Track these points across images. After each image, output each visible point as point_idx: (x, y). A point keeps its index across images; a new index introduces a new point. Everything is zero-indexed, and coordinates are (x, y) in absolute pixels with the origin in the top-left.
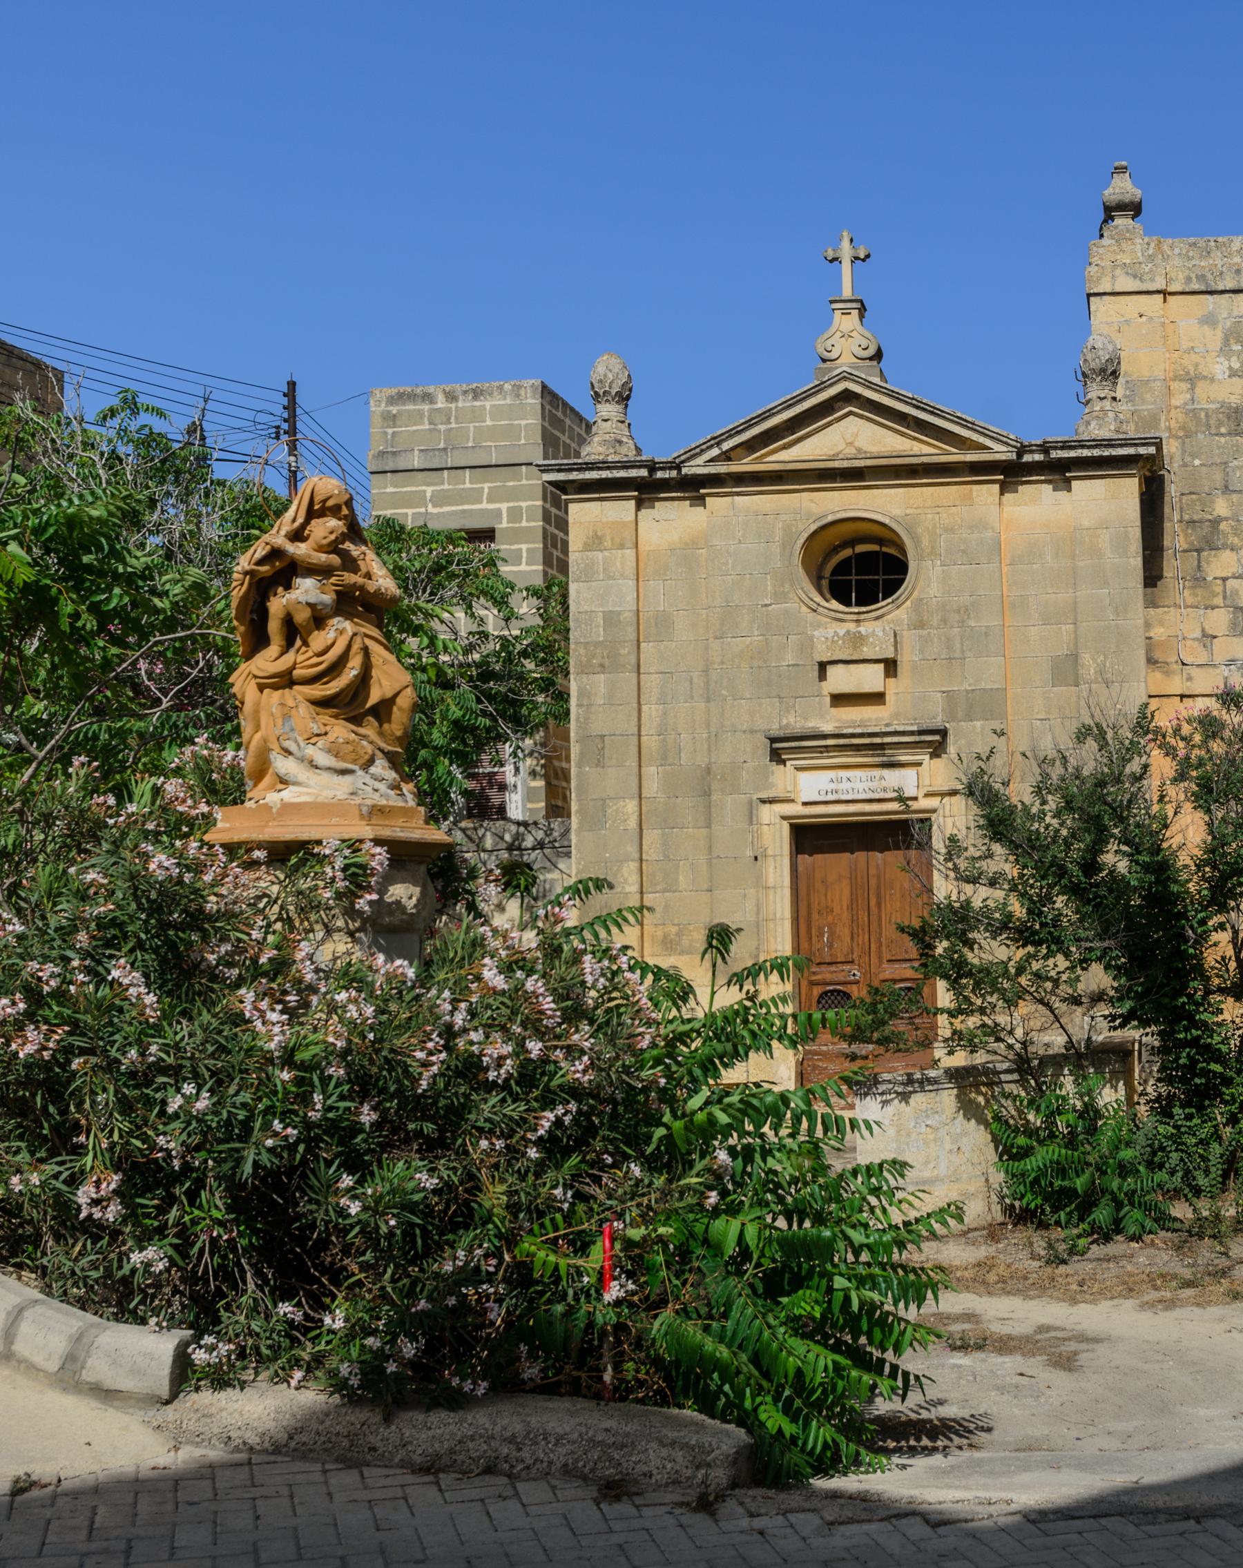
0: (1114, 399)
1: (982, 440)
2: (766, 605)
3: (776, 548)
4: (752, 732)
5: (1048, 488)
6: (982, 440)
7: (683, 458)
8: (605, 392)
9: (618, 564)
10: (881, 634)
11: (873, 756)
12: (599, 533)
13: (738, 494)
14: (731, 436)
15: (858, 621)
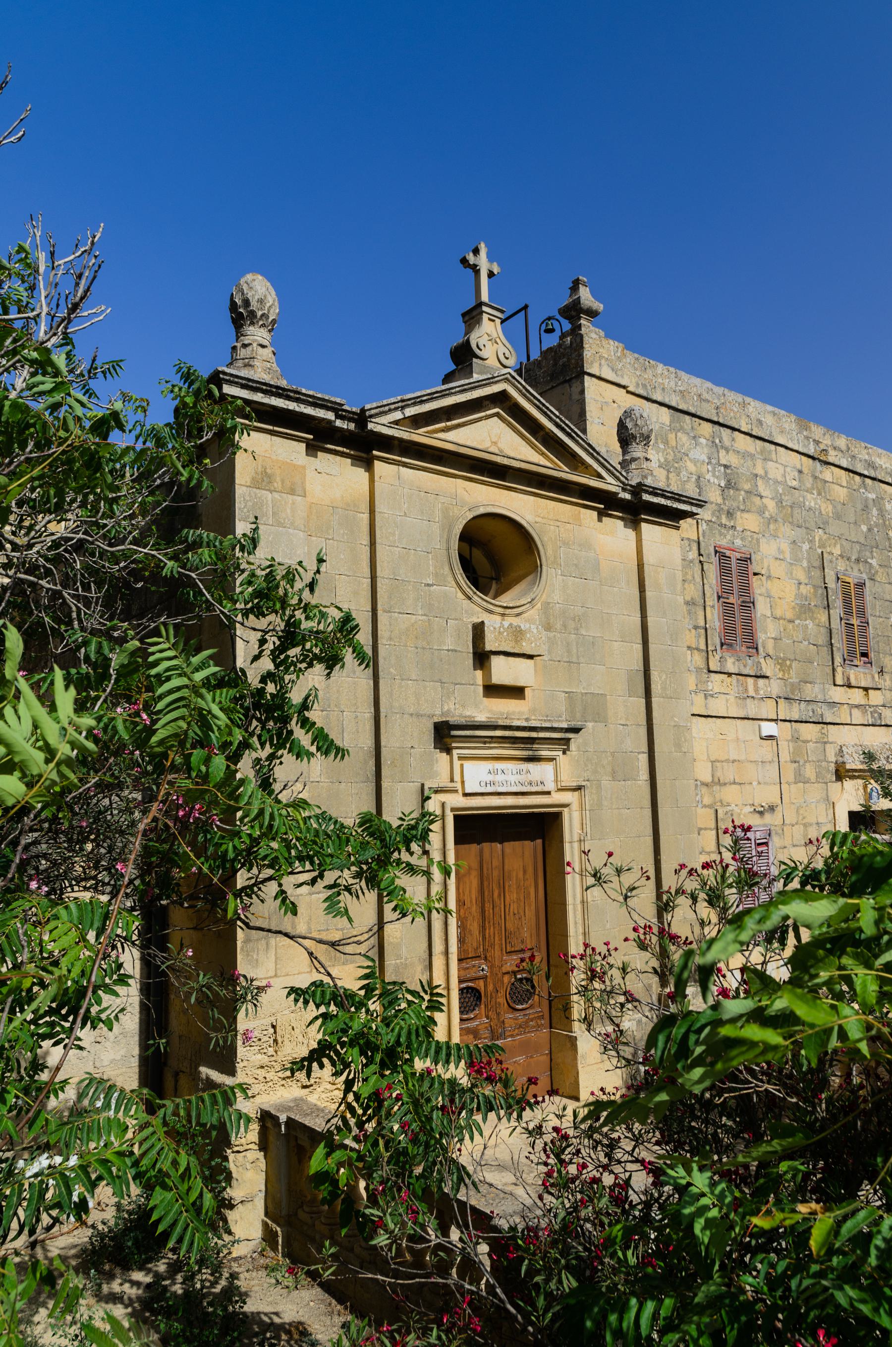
0: (647, 459)
1: (600, 470)
2: (428, 585)
3: (436, 528)
4: (419, 715)
5: (620, 523)
6: (600, 470)
7: (373, 412)
8: (263, 315)
9: (289, 511)
10: (535, 631)
11: (523, 749)
12: (269, 471)
13: (405, 465)
14: (414, 404)
15: (503, 615)
